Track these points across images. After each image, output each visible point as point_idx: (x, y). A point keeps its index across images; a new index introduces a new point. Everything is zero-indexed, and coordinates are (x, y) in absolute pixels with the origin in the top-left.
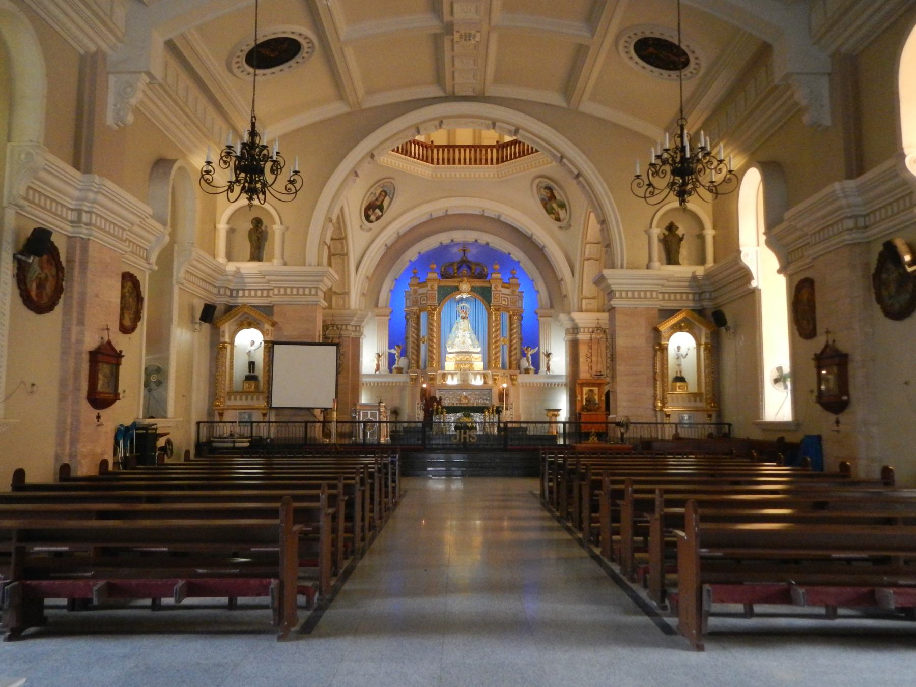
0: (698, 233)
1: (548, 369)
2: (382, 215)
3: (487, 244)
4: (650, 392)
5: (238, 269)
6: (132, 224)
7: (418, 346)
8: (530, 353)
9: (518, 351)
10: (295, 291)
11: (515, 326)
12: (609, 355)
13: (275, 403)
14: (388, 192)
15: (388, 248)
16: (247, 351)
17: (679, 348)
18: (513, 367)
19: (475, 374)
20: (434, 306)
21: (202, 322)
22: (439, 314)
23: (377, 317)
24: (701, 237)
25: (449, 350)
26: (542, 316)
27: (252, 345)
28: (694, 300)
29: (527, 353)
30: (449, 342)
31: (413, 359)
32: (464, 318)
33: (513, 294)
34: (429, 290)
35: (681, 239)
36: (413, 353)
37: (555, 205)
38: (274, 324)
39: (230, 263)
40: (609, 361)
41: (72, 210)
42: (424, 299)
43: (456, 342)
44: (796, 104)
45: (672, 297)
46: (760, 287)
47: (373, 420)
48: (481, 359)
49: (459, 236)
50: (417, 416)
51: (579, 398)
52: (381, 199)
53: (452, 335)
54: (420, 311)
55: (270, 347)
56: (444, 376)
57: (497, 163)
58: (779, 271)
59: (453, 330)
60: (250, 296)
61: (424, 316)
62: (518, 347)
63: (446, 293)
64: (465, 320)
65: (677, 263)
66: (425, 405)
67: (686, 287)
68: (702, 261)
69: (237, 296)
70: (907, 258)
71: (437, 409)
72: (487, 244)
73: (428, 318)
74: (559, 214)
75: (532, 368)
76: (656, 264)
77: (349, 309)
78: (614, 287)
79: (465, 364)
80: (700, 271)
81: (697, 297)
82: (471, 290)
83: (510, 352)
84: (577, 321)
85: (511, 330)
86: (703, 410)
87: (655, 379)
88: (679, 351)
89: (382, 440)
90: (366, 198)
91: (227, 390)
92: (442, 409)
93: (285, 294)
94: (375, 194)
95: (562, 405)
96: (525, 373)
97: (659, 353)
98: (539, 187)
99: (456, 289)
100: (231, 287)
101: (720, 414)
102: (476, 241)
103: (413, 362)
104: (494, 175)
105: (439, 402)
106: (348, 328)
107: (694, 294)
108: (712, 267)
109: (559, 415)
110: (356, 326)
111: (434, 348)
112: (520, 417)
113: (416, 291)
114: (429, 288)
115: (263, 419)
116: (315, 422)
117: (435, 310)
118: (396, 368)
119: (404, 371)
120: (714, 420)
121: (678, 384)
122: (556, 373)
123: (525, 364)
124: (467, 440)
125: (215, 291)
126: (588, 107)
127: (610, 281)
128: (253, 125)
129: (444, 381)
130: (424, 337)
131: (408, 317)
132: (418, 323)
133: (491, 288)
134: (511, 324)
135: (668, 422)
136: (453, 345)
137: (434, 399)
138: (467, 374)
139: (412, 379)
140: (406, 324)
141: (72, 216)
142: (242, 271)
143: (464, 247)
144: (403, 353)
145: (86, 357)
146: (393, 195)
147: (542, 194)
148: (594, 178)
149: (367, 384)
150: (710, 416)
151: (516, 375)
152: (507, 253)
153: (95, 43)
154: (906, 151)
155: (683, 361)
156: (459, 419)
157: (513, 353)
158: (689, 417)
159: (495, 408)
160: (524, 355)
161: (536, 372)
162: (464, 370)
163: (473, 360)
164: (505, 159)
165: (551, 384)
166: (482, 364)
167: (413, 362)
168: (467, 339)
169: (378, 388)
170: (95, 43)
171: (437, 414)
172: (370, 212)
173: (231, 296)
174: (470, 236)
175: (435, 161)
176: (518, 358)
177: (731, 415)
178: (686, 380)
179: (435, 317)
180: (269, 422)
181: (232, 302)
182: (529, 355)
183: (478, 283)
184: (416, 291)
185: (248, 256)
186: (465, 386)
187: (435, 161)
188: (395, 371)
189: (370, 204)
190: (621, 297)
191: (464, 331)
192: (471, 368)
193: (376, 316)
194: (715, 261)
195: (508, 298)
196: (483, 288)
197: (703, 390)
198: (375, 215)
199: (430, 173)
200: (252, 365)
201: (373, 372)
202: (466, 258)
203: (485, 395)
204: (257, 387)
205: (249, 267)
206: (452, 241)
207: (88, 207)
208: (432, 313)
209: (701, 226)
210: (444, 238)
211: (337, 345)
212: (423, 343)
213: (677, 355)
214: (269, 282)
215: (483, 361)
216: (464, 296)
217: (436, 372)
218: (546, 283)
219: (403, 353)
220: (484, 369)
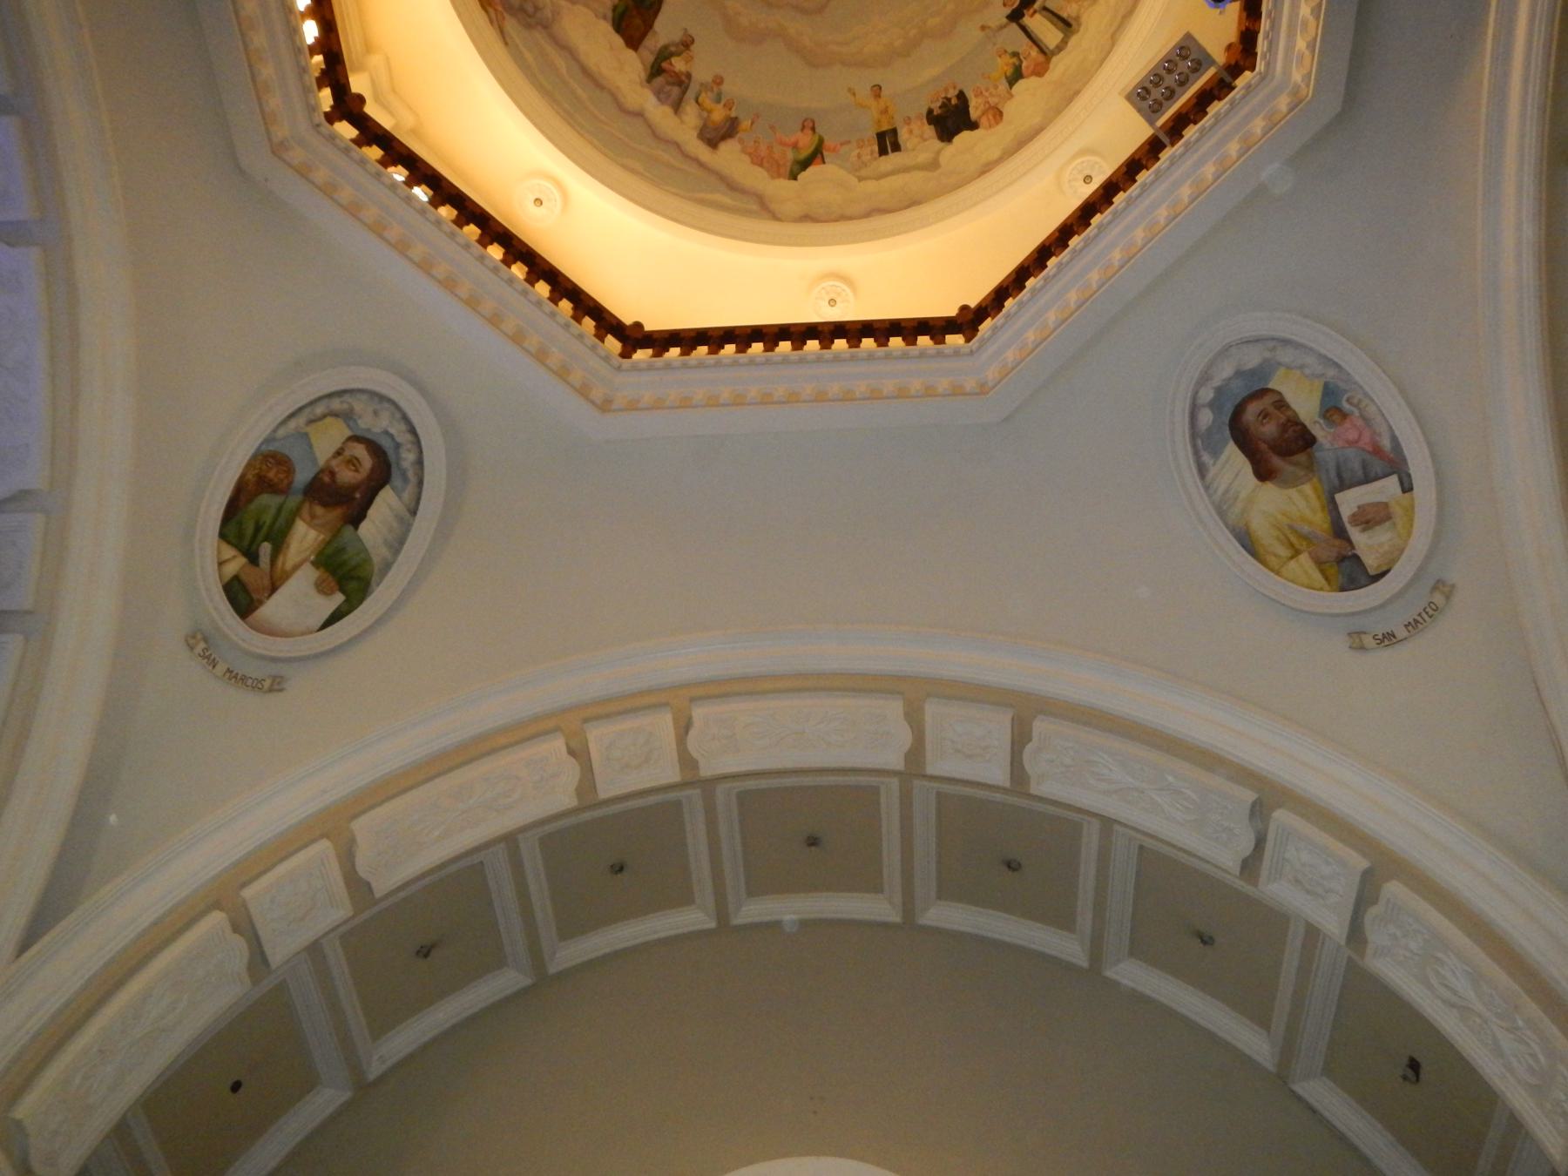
37: (305, 537)
74: (274, 589)
98: (337, 404)
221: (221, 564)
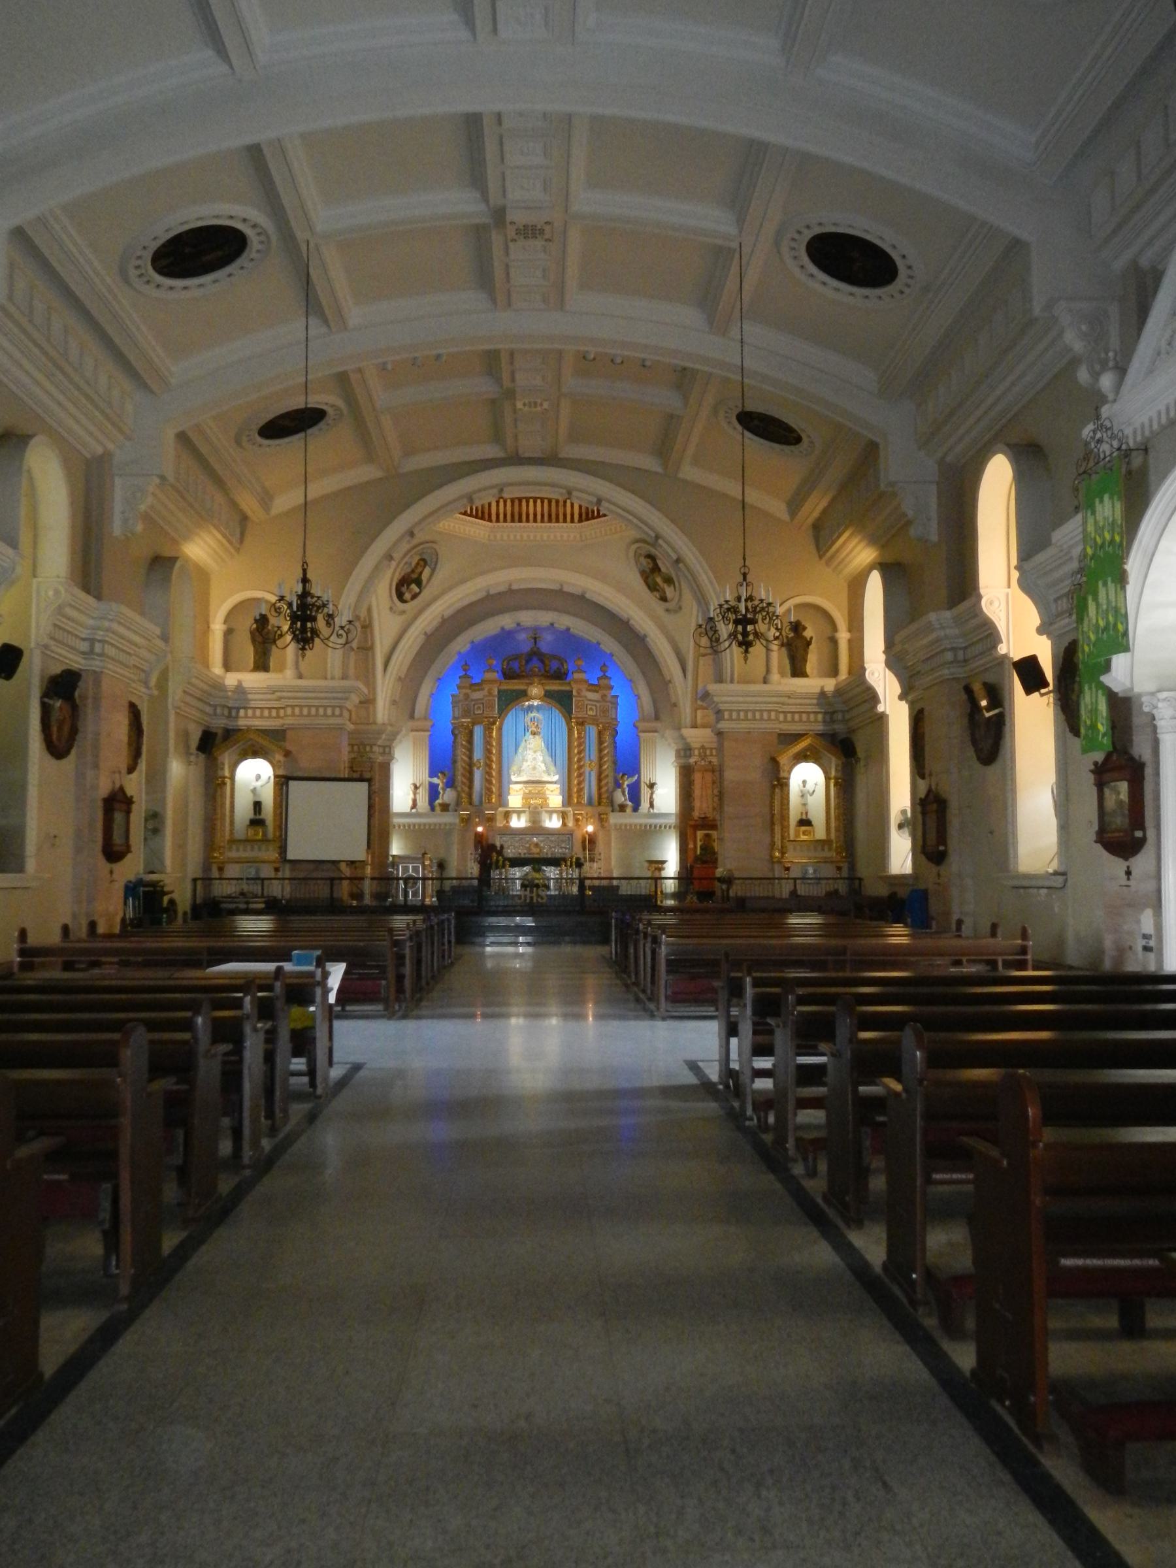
0: (830, 635)
1: (652, 805)
2: (419, 593)
3: (568, 629)
4: (767, 840)
5: (240, 682)
7: (471, 773)
8: (626, 783)
9: (610, 780)
10: (313, 711)
11: (606, 744)
12: (716, 792)
13: (291, 856)
14: (429, 562)
15: (429, 637)
16: (252, 788)
17: (804, 782)
18: (604, 804)
19: (551, 813)
20: (492, 717)
21: (200, 753)
22: (500, 729)
23: (414, 733)
24: (834, 642)
25: (513, 778)
26: (644, 732)
27: (257, 780)
28: (824, 721)
29: (623, 784)
30: (514, 768)
31: (464, 791)
32: (534, 734)
33: (604, 700)
34: (487, 696)
35: (809, 643)
36: (463, 783)
37: (659, 580)
38: (287, 754)
39: (229, 675)
40: (716, 799)
41: (84, 639)
42: (479, 708)
43: (524, 767)
44: (905, 515)
45: (797, 717)
46: (888, 713)
47: (416, 876)
48: (559, 791)
49: (528, 618)
50: (470, 871)
51: (691, 846)
52: (419, 569)
53: (519, 757)
54: (474, 724)
55: (282, 782)
56: (507, 815)
57: (580, 521)
58: (901, 698)
59: (520, 750)
60: (254, 716)
61: (478, 731)
62: (611, 774)
63: (511, 699)
64: (537, 737)
65: (803, 674)
66: (481, 856)
67: (814, 705)
68: (834, 672)
69: (237, 717)
70: (984, 703)
71: (498, 861)
72: (568, 629)
73: (485, 734)
74: (665, 593)
75: (630, 803)
76: (775, 676)
77: (375, 723)
78: (722, 707)
79: (536, 799)
80: (830, 685)
81: (828, 717)
82: (545, 695)
83: (600, 780)
84: (689, 740)
85: (600, 751)
86: (832, 862)
87: (772, 824)
88: (804, 786)
89: (428, 901)
90: (399, 570)
91: (227, 837)
92: (503, 861)
93: (301, 715)
94: (411, 564)
95: (670, 856)
96: (620, 811)
97: (777, 790)
98: (637, 555)
99: (523, 695)
100: (230, 706)
101: (852, 867)
102: (552, 624)
103: (464, 795)
104: (575, 537)
105: (500, 852)
106: (374, 750)
107: (825, 713)
108: (845, 679)
109: (664, 869)
110: (384, 747)
111: (492, 777)
112: (611, 871)
113: (467, 696)
114: (485, 692)
115: (276, 874)
116: (344, 879)
117: (494, 723)
118: (441, 805)
119: (450, 808)
120: (845, 873)
121: (803, 828)
122: (663, 811)
123: (620, 797)
124: (535, 901)
125: (208, 709)
126: (689, 472)
127: (715, 699)
128: (305, 571)
129: (508, 822)
130: (478, 760)
131: (456, 732)
132: (470, 741)
133: (572, 692)
134: (600, 742)
135: (787, 876)
136: (519, 772)
137: (492, 847)
138: (539, 813)
139: (462, 820)
140: (454, 742)
141: (84, 647)
142: (245, 685)
143: (536, 634)
144: (450, 784)
145: (100, 804)
146: (436, 564)
147: (641, 564)
148: (698, 567)
149: (399, 827)
150: (839, 868)
151: (607, 814)
152: (595, 641)
153: (101, 444)
154: (982, 591)
155: (810, 800)
156: (527, 874)
157: (603, 783)
158: (815, 871)
159: (574, 860)
160: (618, 785)
161: (636, 809)
162: (536, 808)
163: (547, 792)
164: (590, 516)
165: (655, 827)
166: (561, 797)
167: (464, 795)
168: (540, 764)
169: (415, 833)
170: (101, 444)
171: (497, 868)
172: (404, 589)
173: (229, 716)
174: (544, 618)
175: (494, 517)
176: (611, 790)
177: (863, 871)
178: (813, 823)
179: (494, 734)
180: (284, 879)
181: (231, 724)
182: (625, 786)
183: (555, 686)
184: (467, 696)
185: (252, 665)
186: (536, 829)
187: (494, 517)
188: (438, 809)
189: (403, 577)
190: (731, 719)
191: (535, 752)
192: (544, 805)
193: (412, 731)
194: (850, 673)
195: (596, 706)
197: (833, 836)
198: (410, 592)
199: (487, 534)
200: (257, 805)
201: (408, 810)
202: (538, 648)
203: (563, 841)
204: (265, 834)
205: (252, 680)
206: (518, 624)
207: (107, 636)
208: (489, 728)
209: (835, 629)
210: (506, 621)
211: (369, 781)
212: (478, 768)
213: (802, 791)
214: (279, 699)
215: (562, 793)
216: (536, 703)
217: (496, 809)
218: (649, 684)
219: (450, 784)
220: (563, 806)
221: (656, 597)
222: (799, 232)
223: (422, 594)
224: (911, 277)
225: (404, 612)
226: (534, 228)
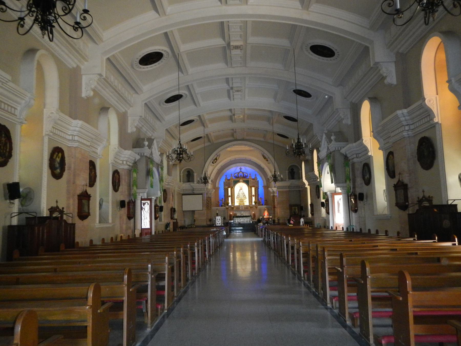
6: (92, 139)
61: (229, 189)
84: (274, 190)
110: (210, 194)
154: (315, 170)
196: (247, 180)
222: (308, 45)
223: (217, 162)
224: (339, 55)
225: (213, 166)
226: (237, 92)
